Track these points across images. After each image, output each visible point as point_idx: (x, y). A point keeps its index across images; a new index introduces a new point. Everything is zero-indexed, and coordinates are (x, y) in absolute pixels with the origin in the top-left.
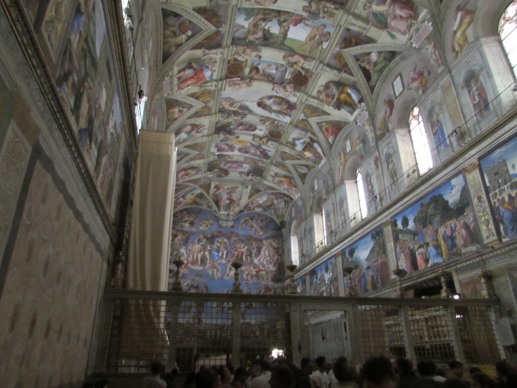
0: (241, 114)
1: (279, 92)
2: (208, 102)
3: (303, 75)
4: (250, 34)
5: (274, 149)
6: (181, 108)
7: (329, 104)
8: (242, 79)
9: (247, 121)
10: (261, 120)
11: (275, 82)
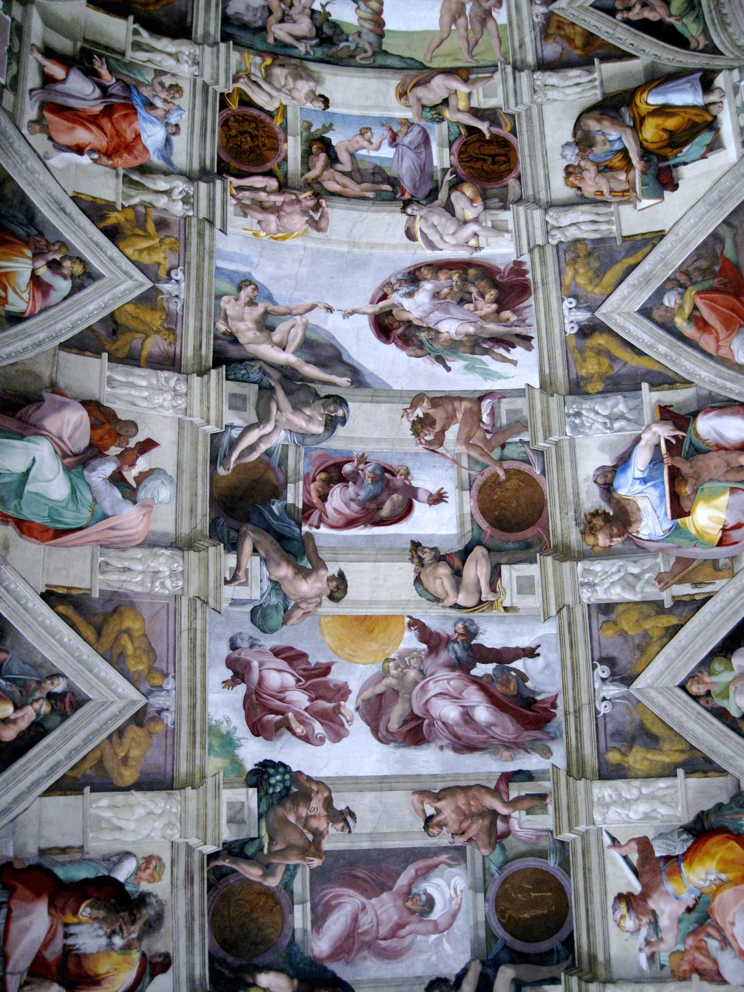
0: (317, 396)
1: (434, 237)
2: (162, 274)
3: (488, 136)
4: (272, 19)
5: (547, 617)
6: (44, 272)
7: (626, 196)
8: (283, 187)
9: (357, 449)
10: (420, 426)
11: (407, 196)
